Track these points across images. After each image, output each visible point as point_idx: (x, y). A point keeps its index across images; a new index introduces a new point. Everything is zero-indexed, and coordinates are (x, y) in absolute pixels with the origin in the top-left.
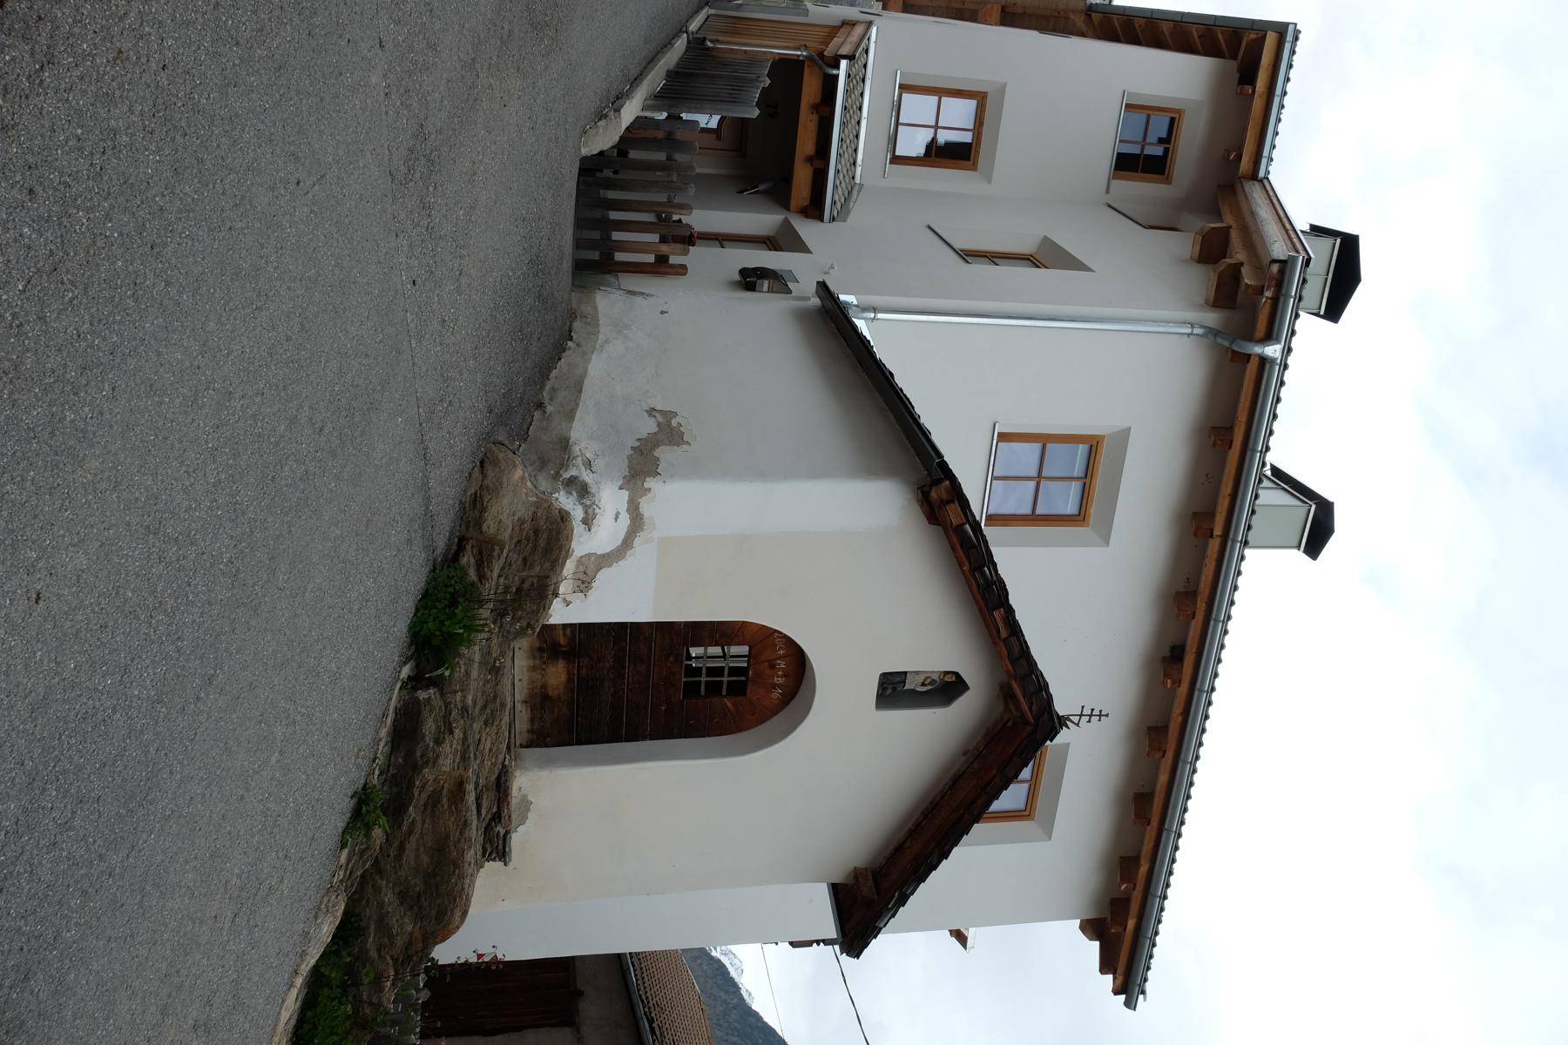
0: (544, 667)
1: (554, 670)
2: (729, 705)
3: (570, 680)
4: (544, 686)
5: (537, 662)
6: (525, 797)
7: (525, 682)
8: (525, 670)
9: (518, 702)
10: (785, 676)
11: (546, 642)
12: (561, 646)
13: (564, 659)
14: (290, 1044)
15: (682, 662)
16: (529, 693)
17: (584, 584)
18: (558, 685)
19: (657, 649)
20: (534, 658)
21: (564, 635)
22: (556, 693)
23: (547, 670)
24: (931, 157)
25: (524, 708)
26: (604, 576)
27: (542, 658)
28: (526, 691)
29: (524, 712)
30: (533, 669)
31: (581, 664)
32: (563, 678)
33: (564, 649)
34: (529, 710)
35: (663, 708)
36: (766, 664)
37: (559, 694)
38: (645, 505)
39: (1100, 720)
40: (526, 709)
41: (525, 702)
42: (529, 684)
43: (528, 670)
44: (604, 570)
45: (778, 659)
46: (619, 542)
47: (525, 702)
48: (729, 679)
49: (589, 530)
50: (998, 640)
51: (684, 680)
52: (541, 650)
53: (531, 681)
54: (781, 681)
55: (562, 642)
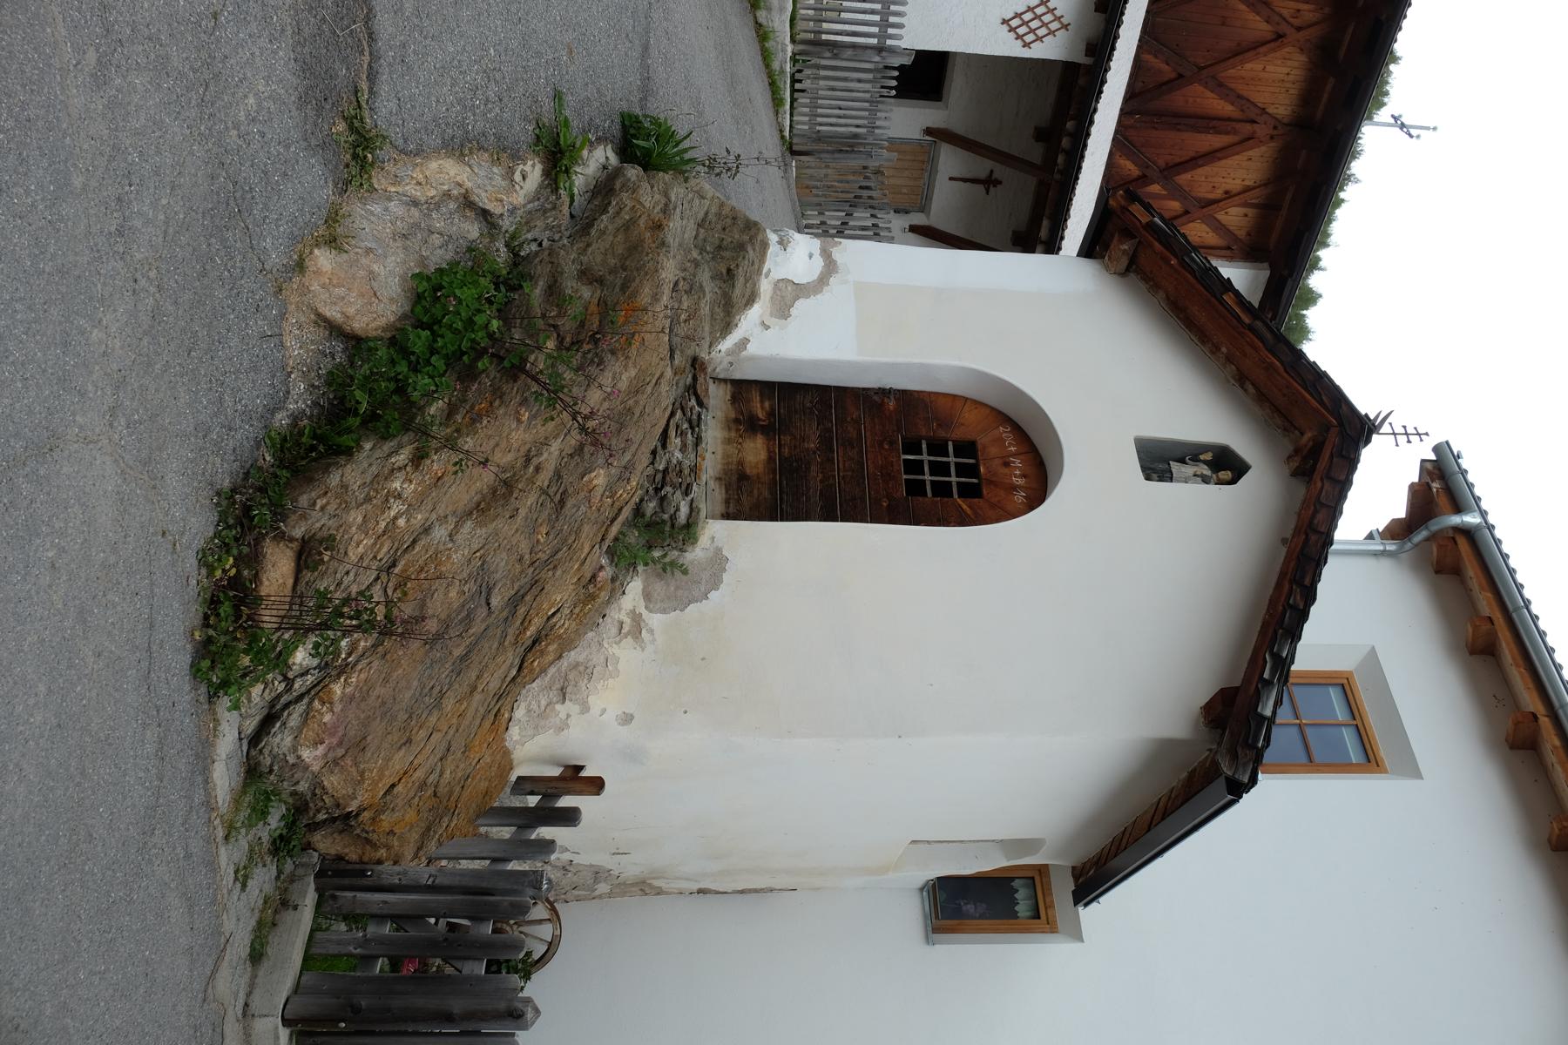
0: (740, 440)
1: (752, 445)
2: (965, 507)
3: (770, 459)
4: (741, 463)
5: (733, 434)
6: (719, 551)
7: (719, 456)
8: (719, 441)
9: (711, 477)
10: (1024, 476)
11: (742, 413)
12: (760, 420)
13: (762, 434)
14: (300, 1024)
15: (900, 457)
16: (724, 469)
17: (782, 309)
18: (757, 463)
19: (868, 434)
20: (730, 429)
21: (762, 408)
22: (755, 471)
23: (744, 444)
24: (1052, 247)
25: (718, 486)
26: (801, 306)
27: (739, 430)
28: (719, 466)
29: (717, 490)
30: (728, 441)
31: (783, 442)
32: (763, 455)
33: (764, 423)
34: (724, 491)
35: (885, 504)
36: (997, 462)
37: (758, 474)
38: (837, 254)
39: (1427, 434)
40: (720, 487)
41: (719, 479)
42: (723, 458)
43: (723, 443)
44: (801, 301)
45: (1011, 456)
46: (815, 277)
47: (719, 479)
48: (954, 484)
49: (785, 250)
50: (1243, 330)
51: (905, 477)
52: (737, 421)
53: (726, 456)
54: (1020, 481)
55: (760, 416)
